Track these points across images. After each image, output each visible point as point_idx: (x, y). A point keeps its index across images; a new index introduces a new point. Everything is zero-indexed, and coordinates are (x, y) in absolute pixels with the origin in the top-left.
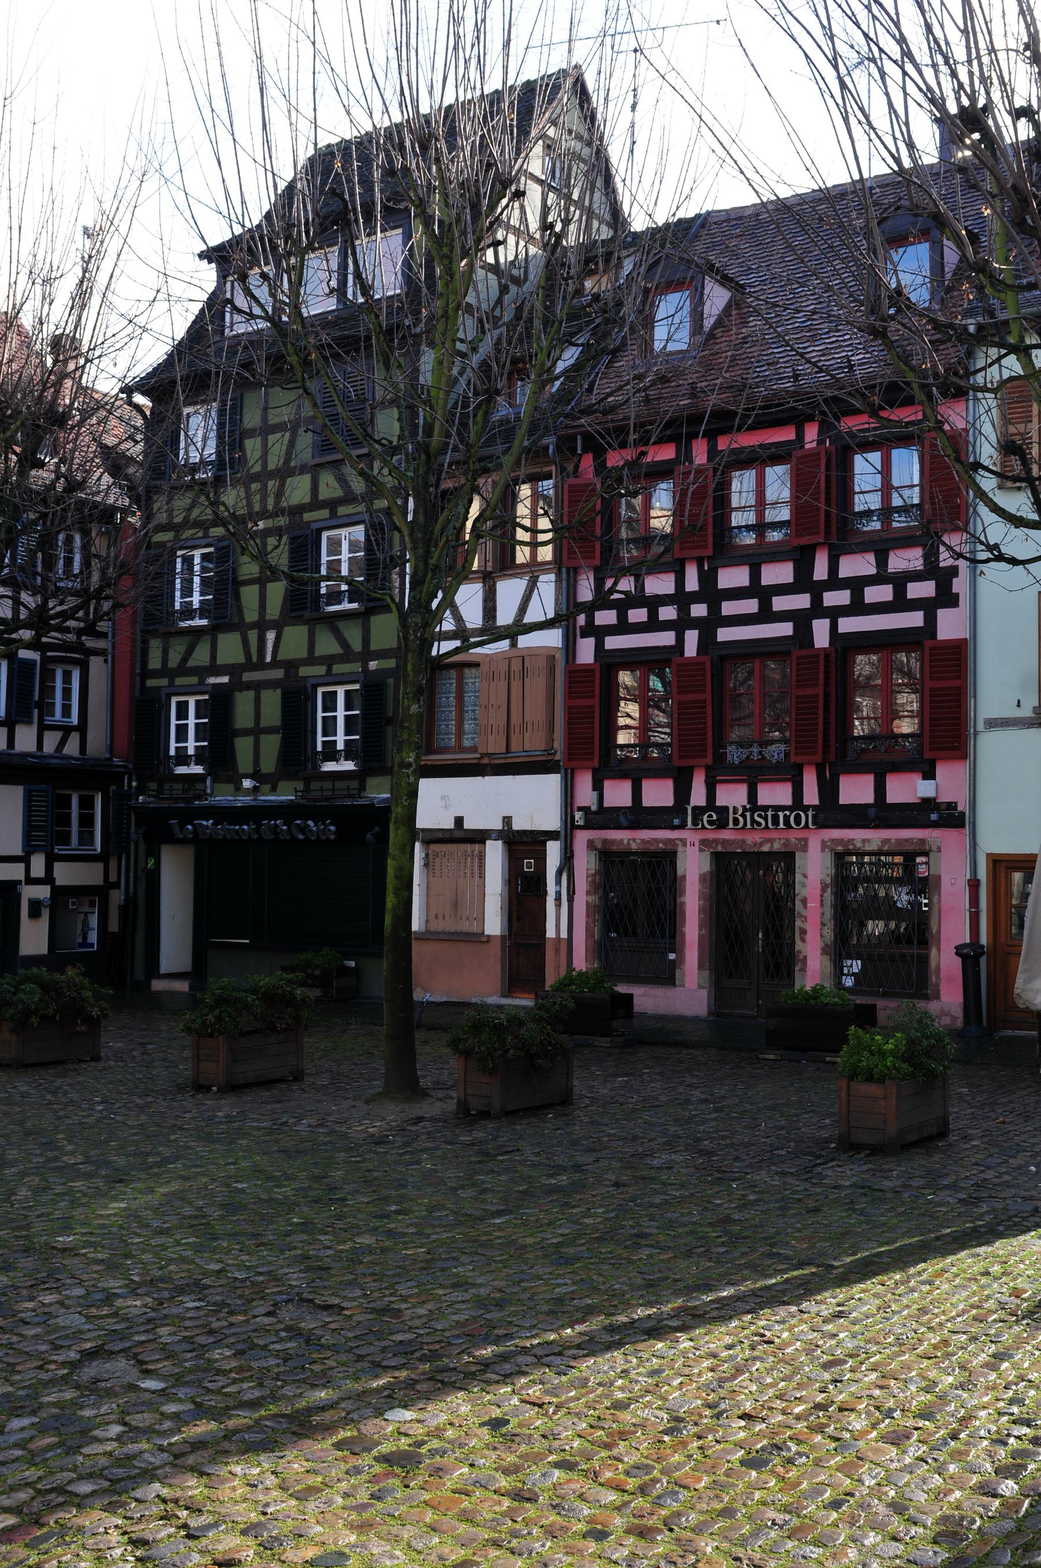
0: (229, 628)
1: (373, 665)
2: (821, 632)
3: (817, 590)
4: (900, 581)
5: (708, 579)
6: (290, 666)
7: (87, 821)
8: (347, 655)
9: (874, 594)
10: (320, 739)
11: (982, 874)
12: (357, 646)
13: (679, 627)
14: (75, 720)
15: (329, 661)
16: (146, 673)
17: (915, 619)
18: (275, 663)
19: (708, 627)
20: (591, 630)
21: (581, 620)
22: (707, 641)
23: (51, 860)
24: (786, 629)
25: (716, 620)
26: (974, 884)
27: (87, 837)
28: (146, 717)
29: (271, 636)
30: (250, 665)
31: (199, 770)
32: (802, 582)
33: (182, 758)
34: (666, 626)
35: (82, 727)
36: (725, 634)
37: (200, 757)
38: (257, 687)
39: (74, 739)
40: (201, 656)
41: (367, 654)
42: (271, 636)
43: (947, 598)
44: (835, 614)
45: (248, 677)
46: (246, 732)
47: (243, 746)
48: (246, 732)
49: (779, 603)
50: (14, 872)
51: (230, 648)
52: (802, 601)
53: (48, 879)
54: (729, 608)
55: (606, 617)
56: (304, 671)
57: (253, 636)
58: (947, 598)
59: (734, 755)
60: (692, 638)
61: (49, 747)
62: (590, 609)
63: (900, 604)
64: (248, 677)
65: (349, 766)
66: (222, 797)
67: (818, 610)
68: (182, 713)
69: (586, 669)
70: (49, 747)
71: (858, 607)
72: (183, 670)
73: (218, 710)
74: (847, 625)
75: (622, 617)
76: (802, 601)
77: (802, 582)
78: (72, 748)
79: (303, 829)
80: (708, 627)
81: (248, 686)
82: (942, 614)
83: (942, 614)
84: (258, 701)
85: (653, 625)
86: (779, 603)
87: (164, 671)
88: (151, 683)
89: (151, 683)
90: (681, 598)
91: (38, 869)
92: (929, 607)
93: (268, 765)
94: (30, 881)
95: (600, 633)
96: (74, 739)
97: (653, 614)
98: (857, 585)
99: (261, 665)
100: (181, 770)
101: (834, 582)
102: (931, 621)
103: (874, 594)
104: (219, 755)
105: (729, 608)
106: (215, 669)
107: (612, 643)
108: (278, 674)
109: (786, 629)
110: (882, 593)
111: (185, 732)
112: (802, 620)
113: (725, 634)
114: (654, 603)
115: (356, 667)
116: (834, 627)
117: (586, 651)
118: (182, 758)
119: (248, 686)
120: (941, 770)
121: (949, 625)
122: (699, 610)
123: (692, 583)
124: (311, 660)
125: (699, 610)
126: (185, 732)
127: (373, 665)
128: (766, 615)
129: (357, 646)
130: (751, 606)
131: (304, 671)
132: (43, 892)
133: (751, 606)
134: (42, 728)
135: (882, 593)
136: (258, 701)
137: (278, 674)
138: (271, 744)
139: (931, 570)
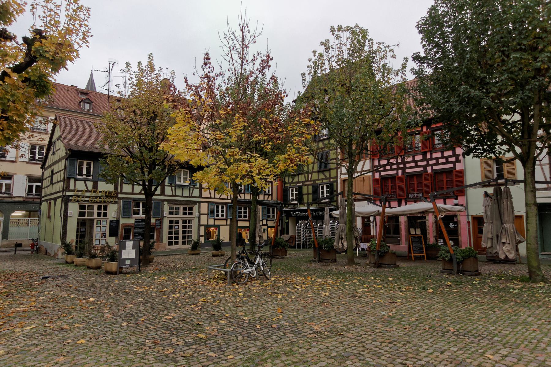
0: (301, 174)
1: (331, 180)
2: (429, 169)
3: (428, 161)
4: (447, 158)
5: (403, 159)
6: (314, 181)
7: (273, 213)
8: (326, 178)
9: (441, 161)
10: (321, 195)
11: (470, 220)
12: (328, 176)
14: (270, 193)
15: (322, 179)
16: (285, 183)
17: (451, 166)
18: (311, 181)
19: (403, 169)
22: (403, 172)
23: (267, 221)
24: (421, 169)
25: (405, 168)
26: (469, 222)
27: (273, 216)
28: (284, 192)
29: (310, 175)
30: (306, 181)
31: (296, 202)
32: (424, 159)
33: (293, 200)
34: (394, 169)
35: (272, 195)
36: (407, 171)
37: (296, 199)
38: (308, 185)
39: (270, 196)
40: (296, 180)
41: (330, 178)
42: (310, 175)
43: (458, 161)
44: (432, 165)
45: (305, 183)
46: (306, 194)
47: (305, 197)
48: (306, 194)
49: (419, 164)
51: (302, 178)
52: (425, 163)
53: (266, 225)
54: (408, 165)
56: (317, 182)
57: (306, 175)
58: (458, 161)
59: (411, 196)
60: (400, 172)
61: (266, 199)
63: (447, 162)
64: (305, 183)
65: (327, 200)
66: (302, 208)
67: (428, 165)
68: (292, 191)
69: (377, 179)
70: (266, 199)
71: (437, 164)
72: (292, 182)
73: (300, 189)
74: (435, 168)
76: (425, 163)
77: (424, 159)
78: (270, 199)
79: (318, 214)
80: (403, 169)
81: (306, 185)
82: (457, 164)
83: (457, 164)
84: (308, 188)
85: (391, 169)
86: (419, 164)
87: (289, 183)
88: (286, 185)
89: (286, 185)
90: (398, 164)
91: (265, 223)
92: (454, 163)
93: (311, 200)
94: (263, 225)
96: (270, 196)
97: (391, 167)
98: (437, 159)
99: (308, 181)
100: (293, 202)
101: (432, 159)
102: (455, 166)
103: (441, 161)
104: (300, 199)
105: (408, 165)
106: (299, 182)
107: (382, 173)
108: (312, 182)
109: (421, 169)
110: (443, 160)
111: (293, 196)
112: (425, 167)
113: (407, 171)
115: (328, 181)
117: (377, 175)
118: (293, 200)
119: (306, 185)
120: (459, 198)
121: (459, 167)
122: (401, 166)
124: (319, 180)
125: (401, 166)
126: (293, 196)
127: (331, 180)
128: (416, 166)
129: (328, 176)
130: (413, 164)
131: (317, 182)
132: (265, 227)
133: (413, 164)
134: (264, 195)
135: (443, 160)
136: (308, 188)
137: (312, 182)
138: (311, 197)
139: (454, 155)
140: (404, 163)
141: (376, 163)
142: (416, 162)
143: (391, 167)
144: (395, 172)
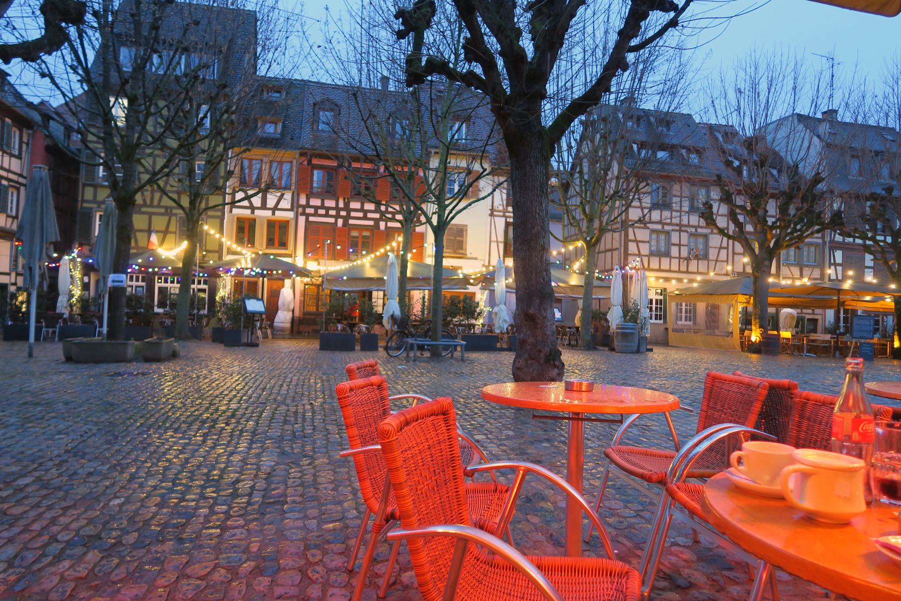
2: (382, 225)
5: (347, 205)
13: (337, 216)
19: (346, 219)
20: (304, 213)
21: (300, 210)
22: (345, 223)
24: (372, 223)
25: (348, 217)
34: (332, 216)
36: (351, 222)
49: (370, 215)
50: (3, 280)
52: (377, 216)
54: (353, 214)
55: (309, 211)
60: (340, 222)
61: (8, 225)
62: (304, 207)
67: (381, 219)
74: (390, 224)
75: (316, 212)
76: (377, 216)
77: (377, 210)
80: (346, 219)
85: (327, 215)
86: (370, 215)
88: (85, 205)
89: (85, 205)
90: (337, 209)
95: (308, 216)
97: (327, 212)
99: (151, 206)
105: (353, 214)
109: (372, 223)
112: (377, 221)
113: (351, 222)
114: (328, 209)
116: (386, 224)
122: (343, 213)
123: (341, 205)
125: (343, 213)
128: (365, 218)
133: (361, 215)
140: (347, 208)
141: (303, 201)
142: (366, 212)
143: (327, 212)
144: (332, 220)
